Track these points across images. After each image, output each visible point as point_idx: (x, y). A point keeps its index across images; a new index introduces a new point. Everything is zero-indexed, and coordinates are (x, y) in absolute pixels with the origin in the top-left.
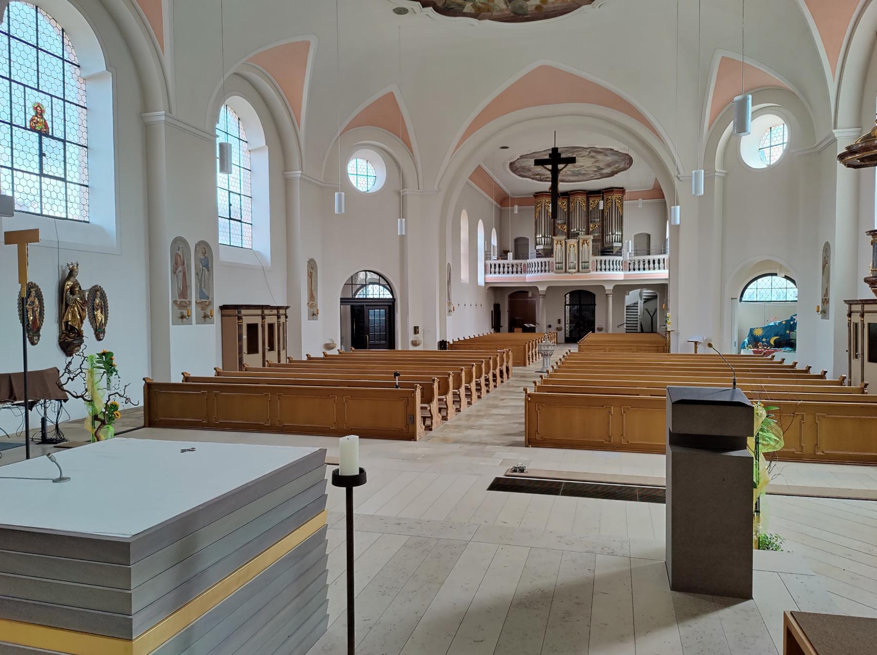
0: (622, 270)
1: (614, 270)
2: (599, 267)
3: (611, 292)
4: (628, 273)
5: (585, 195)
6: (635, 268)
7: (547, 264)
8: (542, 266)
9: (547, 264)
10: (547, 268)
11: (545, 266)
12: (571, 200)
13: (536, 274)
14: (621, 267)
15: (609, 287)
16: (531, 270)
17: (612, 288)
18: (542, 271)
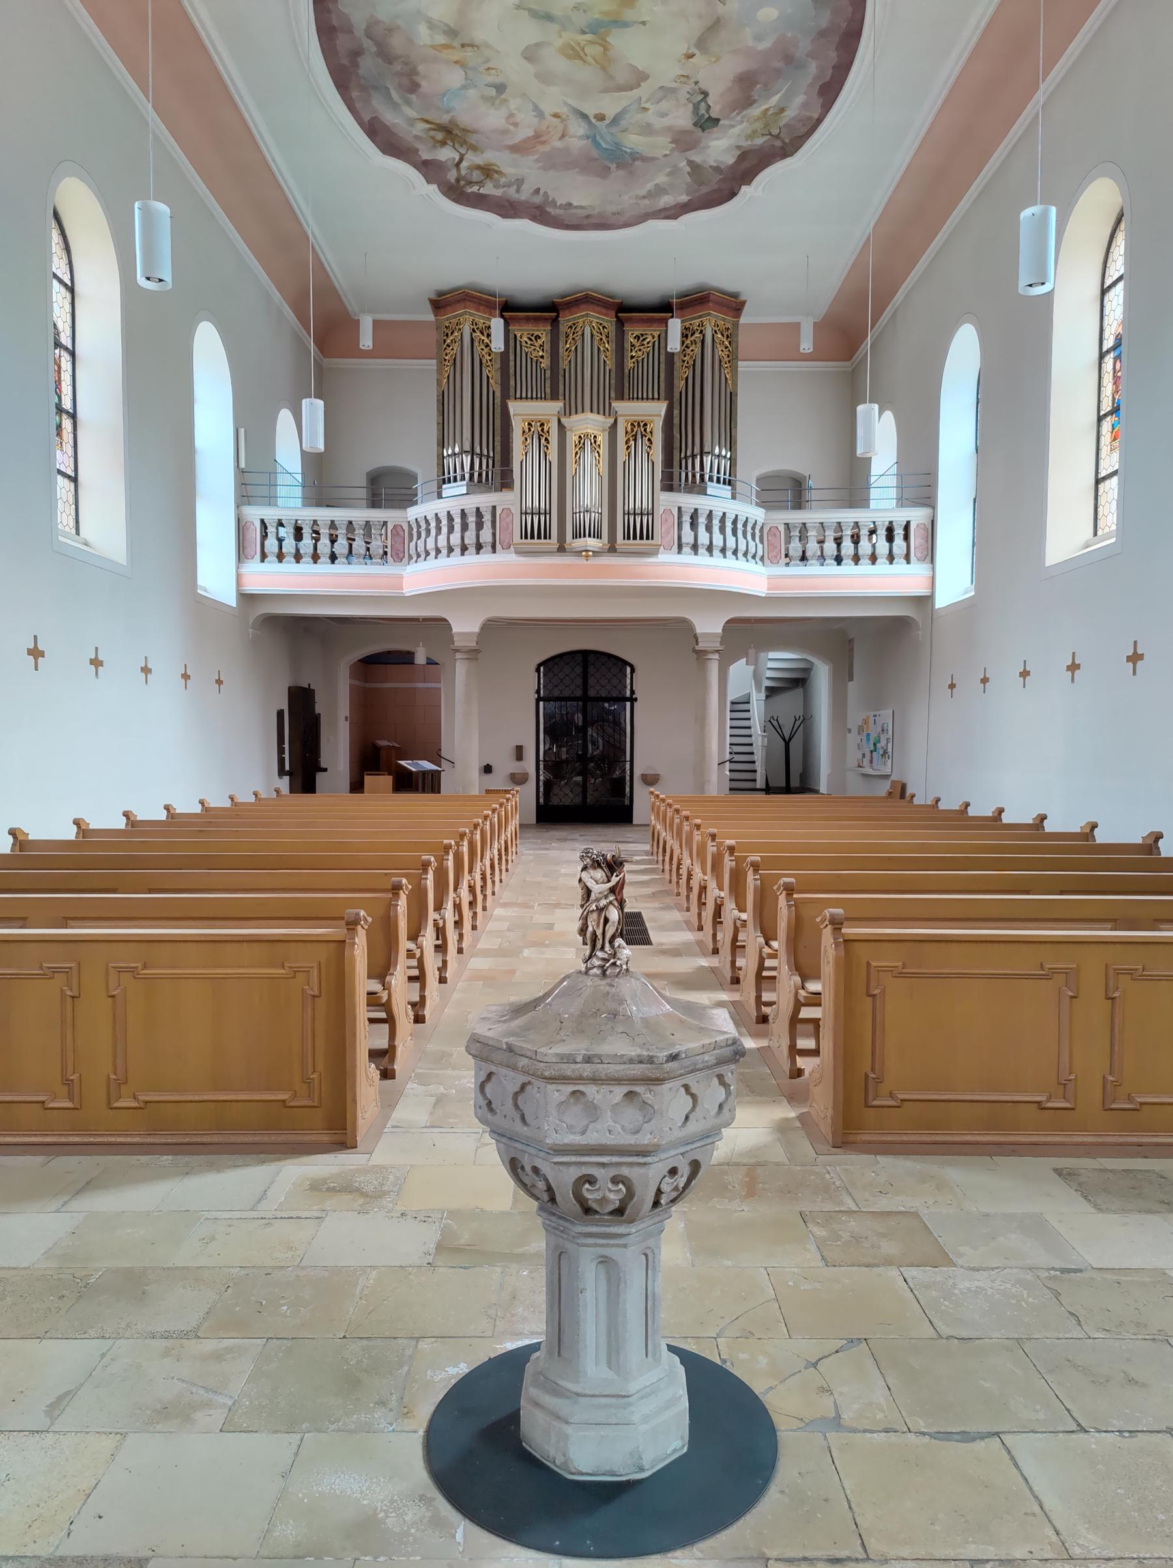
0: (762, 559)
1: (740, 555)
2: (688, 536)
3: (717, 645)
4: (780, 570)
5: (613, 313)
6: (808, 554)
7: (487, 518)
8: (465, 527)
9: (487, 518)
10: (486, 536)
11: (480, 525)
12: (563, 328)
14: (760, 546)
15: (709, 625)
16: (421, 549)
17: (720, 630)
18: (464, 549)
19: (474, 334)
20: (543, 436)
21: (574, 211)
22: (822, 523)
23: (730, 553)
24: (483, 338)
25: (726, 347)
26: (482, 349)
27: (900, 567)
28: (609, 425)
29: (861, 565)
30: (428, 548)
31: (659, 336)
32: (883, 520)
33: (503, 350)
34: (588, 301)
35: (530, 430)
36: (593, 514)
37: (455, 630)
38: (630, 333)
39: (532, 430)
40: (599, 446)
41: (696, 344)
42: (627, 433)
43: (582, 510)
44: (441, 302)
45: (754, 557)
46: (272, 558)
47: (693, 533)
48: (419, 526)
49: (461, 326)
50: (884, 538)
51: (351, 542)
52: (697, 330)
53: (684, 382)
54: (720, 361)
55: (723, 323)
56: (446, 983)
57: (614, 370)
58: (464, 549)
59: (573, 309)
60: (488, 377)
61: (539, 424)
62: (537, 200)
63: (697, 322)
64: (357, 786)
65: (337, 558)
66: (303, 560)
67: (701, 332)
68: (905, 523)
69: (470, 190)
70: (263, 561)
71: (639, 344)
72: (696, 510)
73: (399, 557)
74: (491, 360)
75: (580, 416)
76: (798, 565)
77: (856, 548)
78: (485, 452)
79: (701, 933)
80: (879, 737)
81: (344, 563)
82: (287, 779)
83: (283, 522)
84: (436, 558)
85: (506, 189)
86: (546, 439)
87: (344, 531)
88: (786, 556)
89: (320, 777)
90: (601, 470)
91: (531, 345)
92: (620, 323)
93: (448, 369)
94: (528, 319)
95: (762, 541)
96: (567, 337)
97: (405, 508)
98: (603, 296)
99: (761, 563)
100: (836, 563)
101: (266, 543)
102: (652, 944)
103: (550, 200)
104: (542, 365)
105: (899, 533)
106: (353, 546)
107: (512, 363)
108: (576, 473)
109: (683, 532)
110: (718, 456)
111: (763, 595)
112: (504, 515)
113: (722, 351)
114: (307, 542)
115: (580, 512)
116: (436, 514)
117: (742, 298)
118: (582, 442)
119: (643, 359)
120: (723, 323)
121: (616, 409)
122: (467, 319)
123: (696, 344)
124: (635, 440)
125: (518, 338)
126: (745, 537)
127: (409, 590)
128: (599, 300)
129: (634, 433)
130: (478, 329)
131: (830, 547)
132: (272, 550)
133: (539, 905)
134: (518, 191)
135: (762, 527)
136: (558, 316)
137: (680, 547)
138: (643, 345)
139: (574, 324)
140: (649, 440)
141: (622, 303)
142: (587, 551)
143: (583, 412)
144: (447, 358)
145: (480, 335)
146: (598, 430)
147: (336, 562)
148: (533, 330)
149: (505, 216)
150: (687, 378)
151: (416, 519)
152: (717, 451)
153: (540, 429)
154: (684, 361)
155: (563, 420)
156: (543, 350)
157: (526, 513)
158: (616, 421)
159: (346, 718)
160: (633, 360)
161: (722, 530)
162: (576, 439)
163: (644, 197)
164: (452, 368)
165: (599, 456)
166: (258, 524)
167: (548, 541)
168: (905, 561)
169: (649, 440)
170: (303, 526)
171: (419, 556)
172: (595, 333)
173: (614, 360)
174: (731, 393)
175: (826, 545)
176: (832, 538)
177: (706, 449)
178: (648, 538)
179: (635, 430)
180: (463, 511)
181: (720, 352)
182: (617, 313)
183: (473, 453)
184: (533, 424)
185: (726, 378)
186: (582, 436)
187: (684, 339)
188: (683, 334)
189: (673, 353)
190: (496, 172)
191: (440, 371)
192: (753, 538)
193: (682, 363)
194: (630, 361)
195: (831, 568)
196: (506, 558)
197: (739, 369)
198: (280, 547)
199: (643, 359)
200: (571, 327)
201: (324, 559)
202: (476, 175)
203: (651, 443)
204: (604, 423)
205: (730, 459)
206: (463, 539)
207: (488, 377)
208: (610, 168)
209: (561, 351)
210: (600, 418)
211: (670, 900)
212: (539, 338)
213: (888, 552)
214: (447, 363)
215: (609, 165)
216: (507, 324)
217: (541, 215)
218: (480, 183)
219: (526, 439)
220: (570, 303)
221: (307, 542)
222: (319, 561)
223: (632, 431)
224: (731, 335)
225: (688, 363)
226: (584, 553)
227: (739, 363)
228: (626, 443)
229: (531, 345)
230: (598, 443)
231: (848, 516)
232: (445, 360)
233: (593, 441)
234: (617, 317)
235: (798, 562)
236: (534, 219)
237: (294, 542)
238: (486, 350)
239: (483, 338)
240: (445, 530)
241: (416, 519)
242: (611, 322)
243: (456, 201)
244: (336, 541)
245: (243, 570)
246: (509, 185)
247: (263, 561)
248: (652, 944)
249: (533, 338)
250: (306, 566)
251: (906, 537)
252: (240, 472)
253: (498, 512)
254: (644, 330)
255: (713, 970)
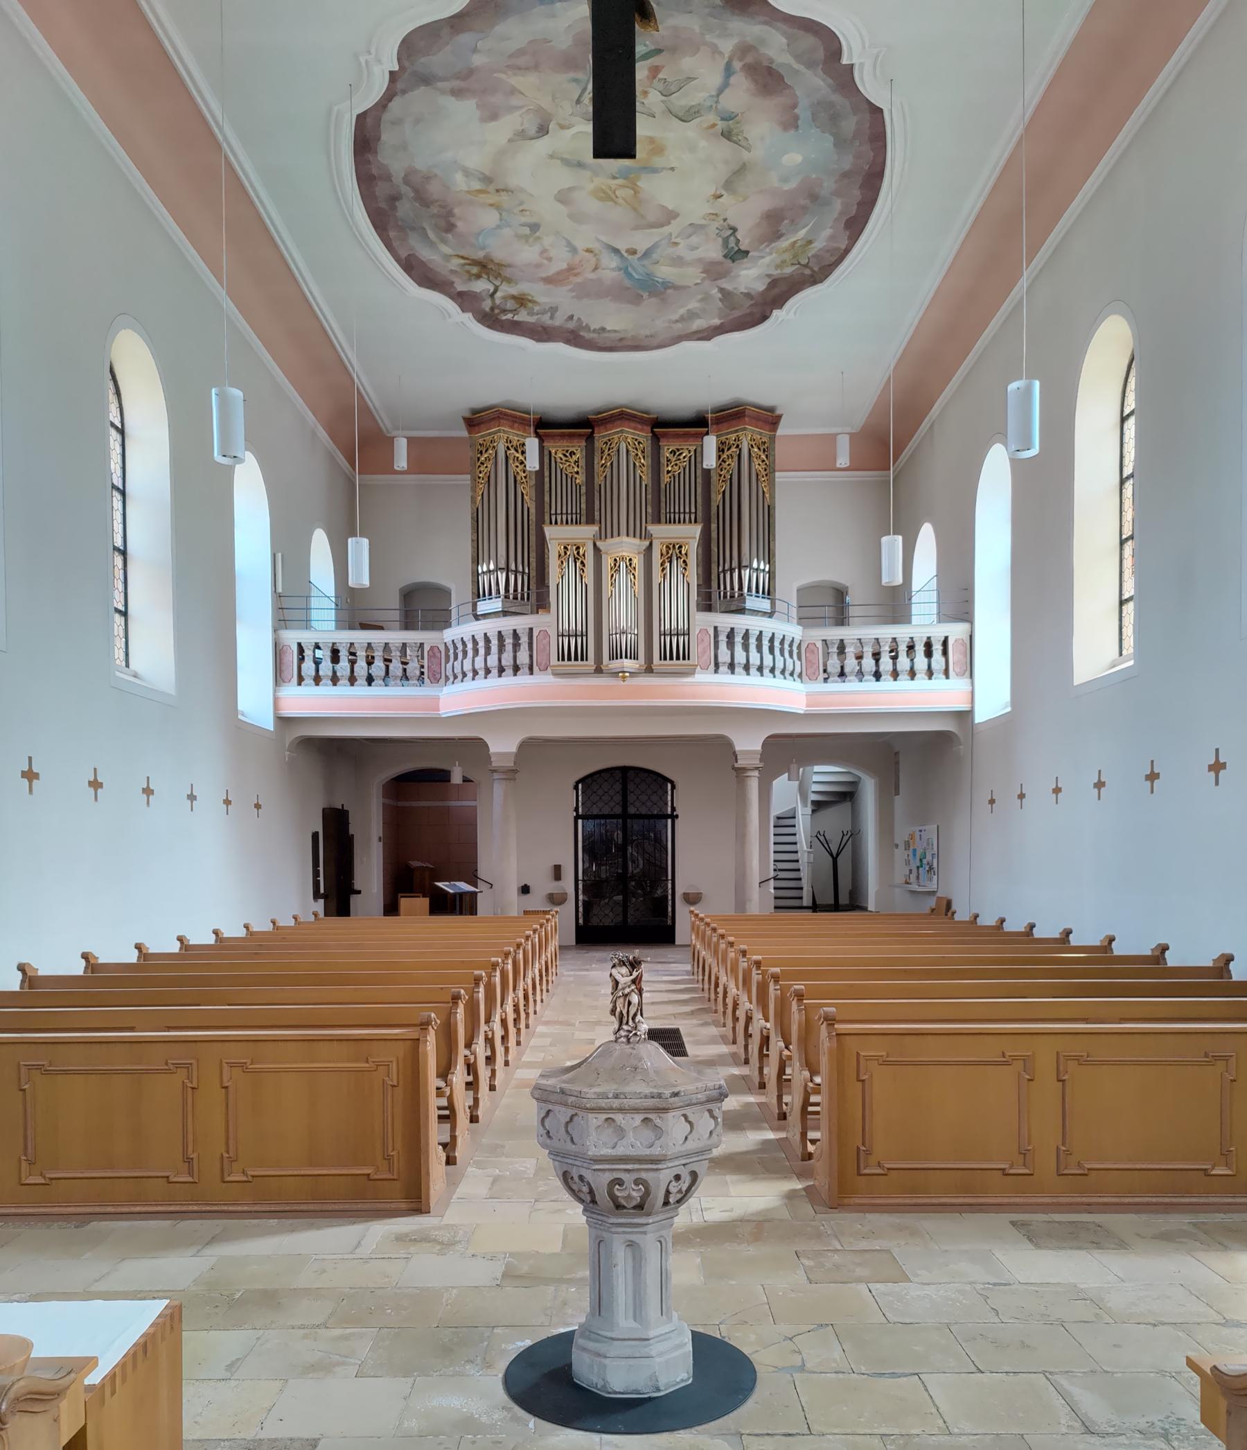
0: (800, 676)
1: (777, 672)
4: (819, 687)
5: (649, 429)
6: (847, 670)
7: (524, 640)
9: (524, 640)
10: (523, 657)
11: (516, 646)
12: (598, 444)
13: (480, 682)
14: (798, 663)
15: (748, 743)
16: (458, 670)
17: (759, 748)
18: (501, 670)
19: (508, 452)
20: (578, 558)
21: (606, 335)
22: (860, 639)
23: (768, 671)
24: (517, 455)
25: (763, 461)
26: (517, 467)
27: (939, 682)
28: (644, 548)
29: (900, 680)
30: (465, 669)
31: (695, 450)
32: (920, 635)
33: (537, 468)
34: (623, 417)
35: (566, 553)
36: (629, 636)
37: (492, 749)
38: (666, 448)
39: (568, 553)
40: (635, 568)
41: (732, 458)
42: (662, 555)
43: (618, 631)
44: (476, 420)
45: (792, 674)
46: (309, 681)
47: (729, 652)
48: (455, 648)
49: (495, 444)
50: (922, 653)
51: (387, 663)
52: (734, 444)
53: (721, 495)
54: (757, 475)
55: (759, 437)
56: (495, 1090)
57: (650, 485)
58: (501, 670)
59: (609, 426)
60: (522, 494)
61: (574, 548)
62: (571, 325)
63: (733, 436)
64: (391, 909)
65: (373, 680)
66: (340, 682)
67: (738, 446)
68: (943, 639)
69: (504, 318)
70: (299, 684)
71: (674, 459)
72: (732, 629)
73: (435, 679)
74: (525, 477)
75: (616, 540)
76: (837, 682)
77: (895, 664)
78: (520, 569)
79: (735, 1046)
80: (925, 853)
81: (381, 686)
82: (321, 901)
83: (320, 645)
84: (473, 679)
85: (539, 316)
86: (582, 563)
87: (381, 653)
88: (825, 671)
89: (354, 899)
90: (636, 591)
91: (566, 461)
92: (656, 438)
93: (482, 487)
94: (563, 436)
95: (799, 658)
96: (602, 453)
97: (441, 629)
98: (636, 411)
99: (799, 680)
100: (874, 679)
101: (304, 666)
102: (688, 1056)
103: (584, 325)
104: (578, 481)
105: (937, 648)
106: (390, 668)
107: (547, 480)
108: (612, 595)
109: (719, 651)
110: (757, 569)
111: (802, 712)
112: (541, 637)
113: (759, 464)
114: (344, 664)
115: (616, 634)
116: (473, 636)
117: (778, 412)
118: (617, 565)
119: (679, 474)
120: (759, 437)
121: (651, 532)
122: (502, 436)
123: (732, 458)
124: (670, 562)
125: (553, 455)
126: (782, 654)
127: (445, 711)
128: (634, 416)
129: (669, 555)
130: (512, 446)
131: (868, 663)
132: (309, 673)
133: (580, 1022)
134: (552, 318)
135: (800, 644)
136: (593, 433)
137: (717, 665)
138: (679, 459)
139: (609, 440)
140: (684, 561)
141: (657, 418)
142: (624, 672)
143: (619, 535)
144: (480, 475)
145: (515, 452)
146: (635, 553)
147: (373, 684)
148: (567, 446)
149: (539, 340)
150: (724, 492)
151: (453, 641)
152: (755, 565)
153: (575, 553)
154: (721, 475)
155: (599, 544)
156: (578, 466)
157: (563, 636)
158: (651, 544)
159: (380, 838)
160: (669, 475)
161: (759, 648)
162: (610, 562)
163: (677, 321)
164: (486, 486)
165: (635, 578)
166: (295, 648)
167: (585, 662)
168: (944, 677)
169: (684, 561)
170: (340, 649)
171: (455, 677)
172: (630, 448)
173: (650, 475)
174: (769, 506)
175: (864, 661)
176: (870, 655)
177: (744, 564)
178: (684, 659)
179: (670, 552)
180: (500, 632)
181: (757, 466)
182: (652, 428)
183: (508, 570)
184: (569, 547)
185: (763, 492)
186: (618, 559)
187: (721, 453)
188: (719, 448)
189: (709, 471)
190: (530, 301)
191: (474, 489)
192: (791, 656)
193: (718, 478)
194: (666, 476)
195: (870, 684)
196: (542, 679)
197: (776, 480)
198: (317, 670)
199: (679, 474)
200: (606, 443)
201: (362, 681)
202: (510, 305)
203: (686, 565)
204: (639, 546)
205: (769, 572)
206: (500, 660)
207: (522, 494)
208: (642, 296)
209: (596, 466)
210: (637, 541)
211: (708, 1017)
212: (574, 454)
213: (926, 667)
214: (481, 480)
215: (642, 293)
216: (541, 440)
217: (574, 339)
218: (514, 311)
219: (562, 562)
220: (606, 419)
221: (344, 664)
222: (356, 683)
223: (668, 553)
224: (767, 449)
225: (724, 477)
226: (620, 674)
227: (777, 474)
228: (662, 565)
229: (566, 461)
230: (633, 565)
231: (886, 632)
232: (479, 478)
233: (628, 564)
234: (652, 432)
235: (837, 678)
236: (568, 342)
237: (331, 665)
238: (521, 467)
239: (517, 455)
240: (482, 651)
241: (453, 641)
242: (647, 436)
243: (489, 327)
244: (373, 663)
245: (280, 694)
246: (544, 313)
247: (299, 684)
248: (688, 1056)
249: (568, 454)
250: (343, 689)
251: (945, 653)
252: (277, 596)
253: (535, 634)
254: (680, 445)
255: (744, 1077)
